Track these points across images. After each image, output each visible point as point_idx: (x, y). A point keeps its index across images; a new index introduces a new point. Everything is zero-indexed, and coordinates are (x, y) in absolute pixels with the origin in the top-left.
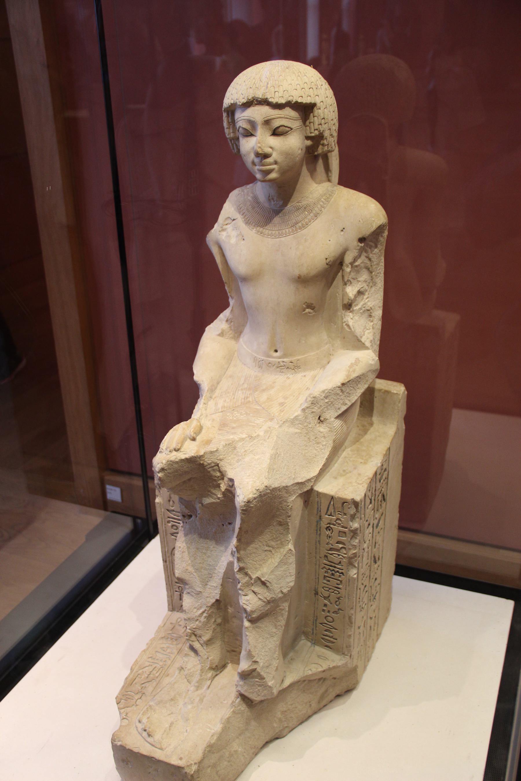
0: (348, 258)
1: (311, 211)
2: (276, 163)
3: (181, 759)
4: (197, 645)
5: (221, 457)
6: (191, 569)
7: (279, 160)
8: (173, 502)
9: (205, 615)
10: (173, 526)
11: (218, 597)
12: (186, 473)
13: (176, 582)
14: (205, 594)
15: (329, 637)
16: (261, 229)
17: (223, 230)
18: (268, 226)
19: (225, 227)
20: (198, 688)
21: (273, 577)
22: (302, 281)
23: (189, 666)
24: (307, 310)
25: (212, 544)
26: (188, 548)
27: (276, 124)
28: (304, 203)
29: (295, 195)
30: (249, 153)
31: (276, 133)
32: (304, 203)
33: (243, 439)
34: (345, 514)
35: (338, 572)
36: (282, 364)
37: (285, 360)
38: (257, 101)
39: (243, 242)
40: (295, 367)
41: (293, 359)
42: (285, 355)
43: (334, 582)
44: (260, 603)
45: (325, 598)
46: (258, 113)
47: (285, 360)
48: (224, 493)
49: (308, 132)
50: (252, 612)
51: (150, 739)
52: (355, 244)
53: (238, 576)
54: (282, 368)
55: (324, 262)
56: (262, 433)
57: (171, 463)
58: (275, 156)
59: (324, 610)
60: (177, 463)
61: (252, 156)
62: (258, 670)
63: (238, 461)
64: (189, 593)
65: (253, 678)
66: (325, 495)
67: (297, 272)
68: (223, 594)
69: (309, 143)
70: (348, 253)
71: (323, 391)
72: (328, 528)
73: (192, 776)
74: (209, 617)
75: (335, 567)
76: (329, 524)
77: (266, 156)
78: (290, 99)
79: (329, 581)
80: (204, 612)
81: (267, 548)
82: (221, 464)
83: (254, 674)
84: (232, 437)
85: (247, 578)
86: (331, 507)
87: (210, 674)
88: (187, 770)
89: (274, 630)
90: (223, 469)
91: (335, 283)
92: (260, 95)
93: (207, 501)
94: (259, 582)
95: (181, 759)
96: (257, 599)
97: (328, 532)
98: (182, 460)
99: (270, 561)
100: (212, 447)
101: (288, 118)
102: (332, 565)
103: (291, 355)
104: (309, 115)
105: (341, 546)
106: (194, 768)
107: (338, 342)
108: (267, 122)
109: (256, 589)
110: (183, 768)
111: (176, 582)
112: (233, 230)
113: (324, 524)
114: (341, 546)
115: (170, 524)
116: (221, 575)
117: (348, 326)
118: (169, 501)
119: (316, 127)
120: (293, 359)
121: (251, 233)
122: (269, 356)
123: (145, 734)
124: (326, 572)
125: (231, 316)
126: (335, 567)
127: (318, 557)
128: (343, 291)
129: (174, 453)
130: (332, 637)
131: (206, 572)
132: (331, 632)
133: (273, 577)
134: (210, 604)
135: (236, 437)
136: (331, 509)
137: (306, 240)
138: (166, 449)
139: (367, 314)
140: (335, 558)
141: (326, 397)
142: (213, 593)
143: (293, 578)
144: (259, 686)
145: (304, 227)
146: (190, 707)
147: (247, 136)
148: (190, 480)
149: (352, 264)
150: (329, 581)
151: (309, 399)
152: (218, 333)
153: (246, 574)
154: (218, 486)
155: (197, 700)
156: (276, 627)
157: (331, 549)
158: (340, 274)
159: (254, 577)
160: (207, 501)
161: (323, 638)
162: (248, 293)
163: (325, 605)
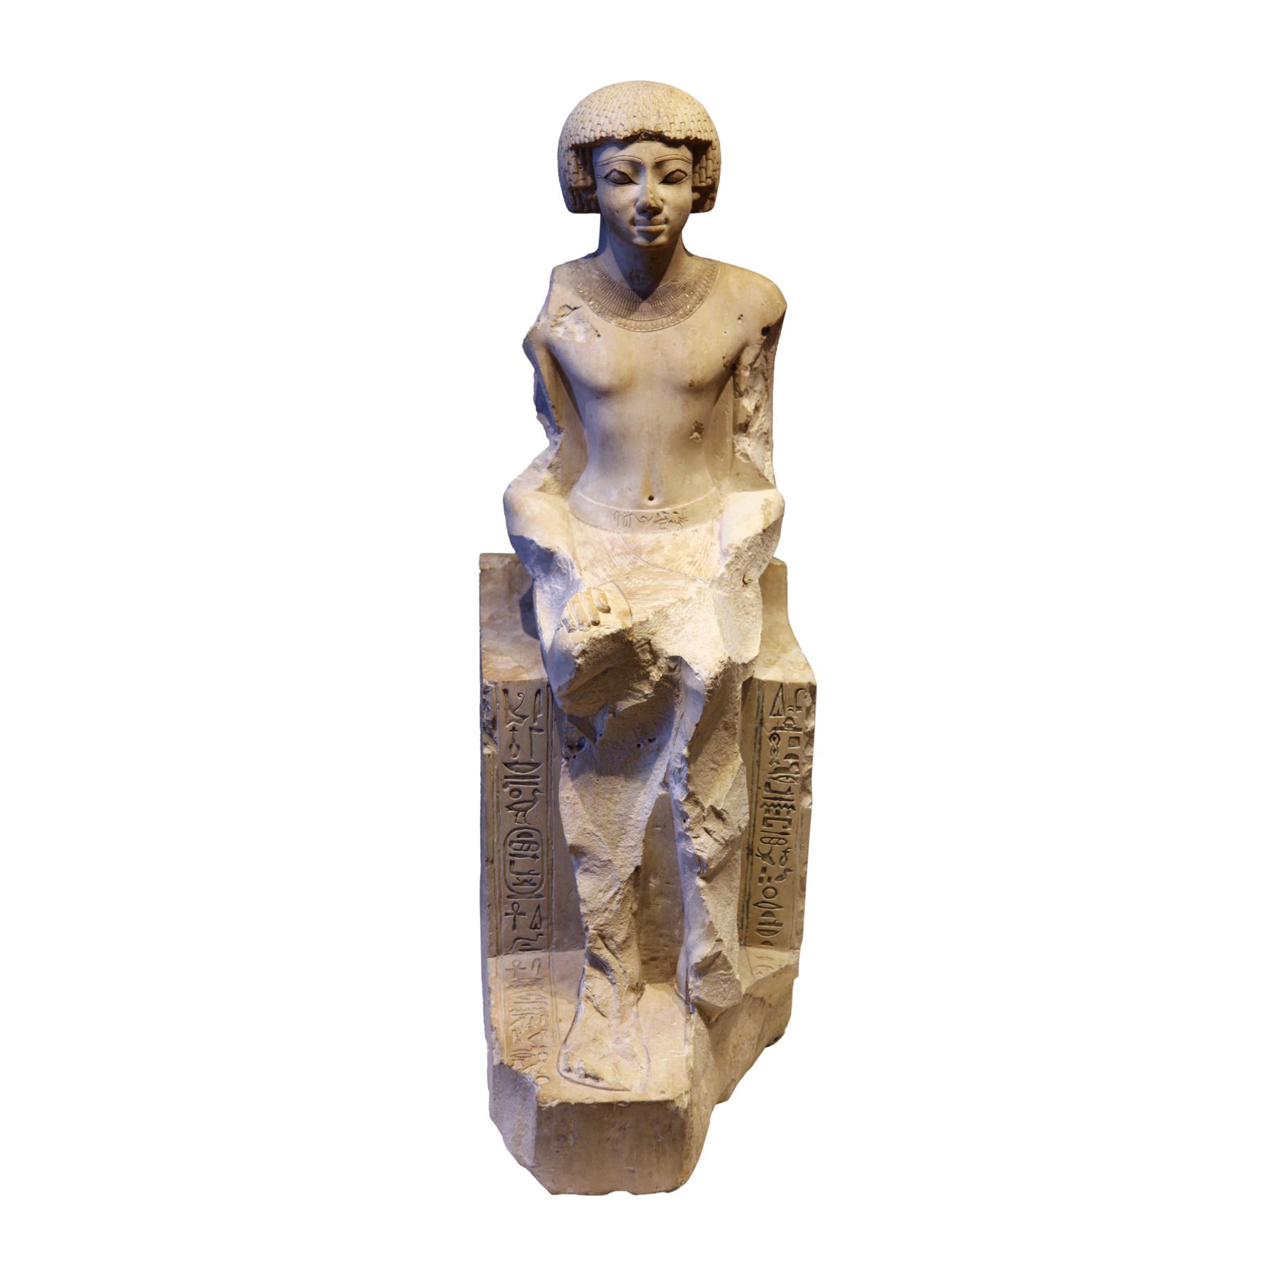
0: (747, 358)
1: (692, 292)
2: (666, 221)
3: (663, 1092)
4: (605, 955)
5: (653, 630)
6: (591, 827)
7: (671, 218)
8: (518, 747)
9: (618, 897)
10: (512, 791)
11: (639, 862)
12: (607, 658)
13: (509, 897)
14: (617, 863)
15: (769, 924)
16: (624, 320)
17: (558, 324)
18: (633, 316)
19: (560, 319)
20: (622, 1019)
21: (728, 804)
22: (694, 389)
23: (597, 992)
24: (696, 434)
25: (618, 783)
26: (581, 796)
27: (671, 167)
28: (681, 281)
29: (670, 270)
30: (626, 208)
31: (668, 180)
32: (681, 281)
33: (673, 605)
34: (799, 708)
35: (786, 806)
36: (662, 516)
37: (666, 509)
38: (646, 134)
39: (598, 339)
40: (680, 520)
41: (678, 507)
42: (667, 503)
43: (778, 826)
44: (716, 846)
45: (764, 856)
46: (647, 152)
47: (666, 509)
48: (657, 686)
49: (697, 181)
50: (710, 860)
51: (600, 1084)
52: (758, 337)
53: (687, 808)
54: (661, 521)
55: (721, 362)
56: (694, 596)
57: (594, 641)
58: (666, 212)
59: (761, 880)
60: (600, 641)
61: (632, 211)
62: (724, 953)
63: (677, 632)
64: (586, 870)
65: (715, 970)
66: (771, 683)
67: (687, 378)
68: (646, 856)
69: (697, 195)
70: (747, 349)
71: (745, 540)
72: (772, 737)
73: (686, 1111)
74: (623, 902)
75: (781, 799)
76: (775, 728)
77: (658, 211)
78: (689, 134)
79: (771, 825)
80: (616, 893)
81: (713, 765)
82: (654, 640)
83: (719, 961)
84: (656, 604)
85: (698, 810)
86: (779, 700)
87: (632, 997)
88: (679, 1104)
89: (730, 895)
90: (657, 647)
91: (722, 395)
92: (651, 126)
93: (625, 705)
94: (712, 814)
95: (663, 1092)
96: (712, 841)
97: (772, 744)
98: (607, 637)
99: (718, 784)
100: (638, 617)
101: (679, 159)
102: (777, 795)
103: (674, 502)
104: (700, 158)
105: (791, 761)
106: (686, 1099)
107: (726, 483)
108: (659, 165)
109: (709, 826)
110: (673, 1101)
111: (509, 897)
112: (577, 323)
113: (766, 732)
114: (791, 761)
115: (507, 790)
116: (643, 825)
117: (746, 456)
118: (511, 746)
119: (710, 173)
120: (678, 507)
121: (611, 328)
122: (641, 506)
123: (588, 1081)
124: (768, 811)
125: (556, 460)
126: (781, 799)
127: (755, 789)
128: (735, 405)
129: (594, 628)
130: (774, 923)
131: (615, 827)
132: (771, 914)
133: (728, 804)
134: (625, 878)
135: (665, 602)
136: (779, 703)
137: (694, 333)
138: (581, 624)
139: (763, 439)
140: (781, 785)
141: (749, 548)
142: (628, 857)
143: (746, 809)
144: (725, 981)
145: (687, 314)
146: (627, 1040)
147: (623, 184)
148: (604, 673)
149: (751, 365)
150: (771, 825)
151: (732, 551)
152: (537, 487)
153: (697, 803)
154: (647, 676)
155: (633, 1031)
156: (730, 888)
157: (776, 770)
158: (730, 382)
159: (707, 806)
160: (625, 705)
161: (758, 930)
162: (607, 416)
163: (764, 869)
